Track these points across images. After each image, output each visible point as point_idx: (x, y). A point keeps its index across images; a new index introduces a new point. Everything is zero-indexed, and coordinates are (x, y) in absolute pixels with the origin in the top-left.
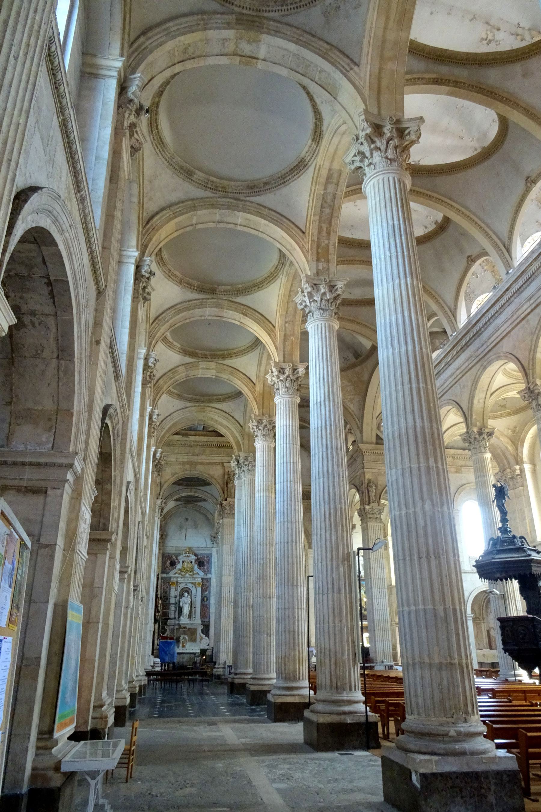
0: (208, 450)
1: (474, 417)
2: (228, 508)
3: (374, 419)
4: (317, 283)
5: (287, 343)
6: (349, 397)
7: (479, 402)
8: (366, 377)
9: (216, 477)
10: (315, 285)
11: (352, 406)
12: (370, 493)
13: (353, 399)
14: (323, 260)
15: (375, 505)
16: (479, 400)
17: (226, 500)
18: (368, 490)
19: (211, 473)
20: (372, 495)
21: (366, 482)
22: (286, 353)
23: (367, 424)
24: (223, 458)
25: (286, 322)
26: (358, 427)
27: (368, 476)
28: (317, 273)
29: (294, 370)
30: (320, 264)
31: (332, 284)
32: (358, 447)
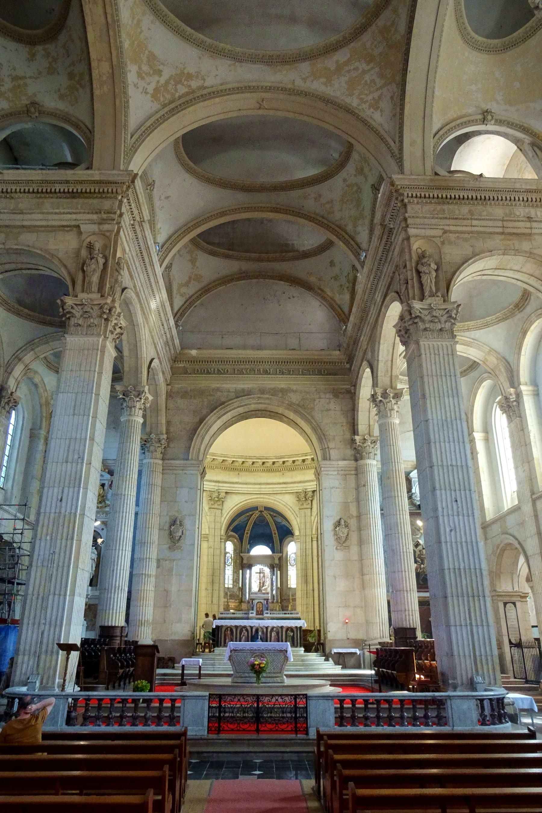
0: (48, 204)
2: (78, 315)
3: (429, 135)
6: (370, 97)
8: (402, 28)
9: (60, 255)
11: (377, 116)
12: (424, 279)
13: (380, 97)
15: (436, 302)
17: (77, 296)
18: (418, 273)
19: (51, 246)
20: (429, 281)
21: (415, 258)
23: (413, 143)
24: (79, 217)
26: (393, 156)
27: (416, 245)
32: (392, 184)
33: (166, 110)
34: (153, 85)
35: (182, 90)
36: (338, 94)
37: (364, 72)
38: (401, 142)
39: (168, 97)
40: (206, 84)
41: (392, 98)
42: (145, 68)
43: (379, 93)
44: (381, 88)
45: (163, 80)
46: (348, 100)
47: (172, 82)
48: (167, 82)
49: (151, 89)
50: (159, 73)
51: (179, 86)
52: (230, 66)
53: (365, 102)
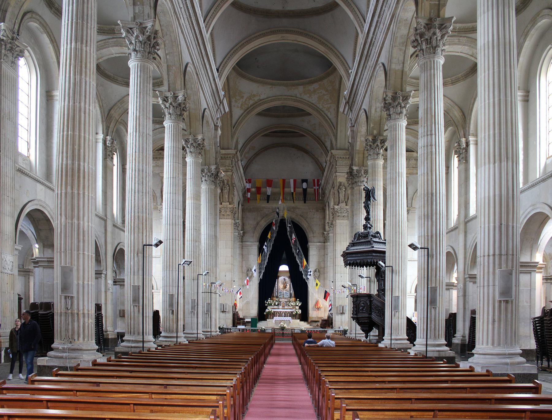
1: (372, 125)
4: (132, 26)
5: (170, 73)
7: (376, 111)
10: (131, 29)
11: (329, 114)
14: (139, 3)
16: (376, 109)
22: (171, 82)
25: (166, 55)
28: (134, 17)
29: (175, 97)
30: (137, 8)
31: (144, 26)
33: (246, 113)
34: (241, 103)
35: (251, 102)
36: (313, 102)
37: (324, 95)
38: (337, 126)
39: (246, 106)
40: (261, 98)
41: (334, 109)
42: (238, 98)
43: (330, 105)
44: (331, 103)
45: (244, 100)
46: (318, 105)
47: (248, 100)
48: (246, 100)
49: (240, 106)
50: (243, 97)
51: (250, 101)
52: (270, 88)
53: (325, 108)
